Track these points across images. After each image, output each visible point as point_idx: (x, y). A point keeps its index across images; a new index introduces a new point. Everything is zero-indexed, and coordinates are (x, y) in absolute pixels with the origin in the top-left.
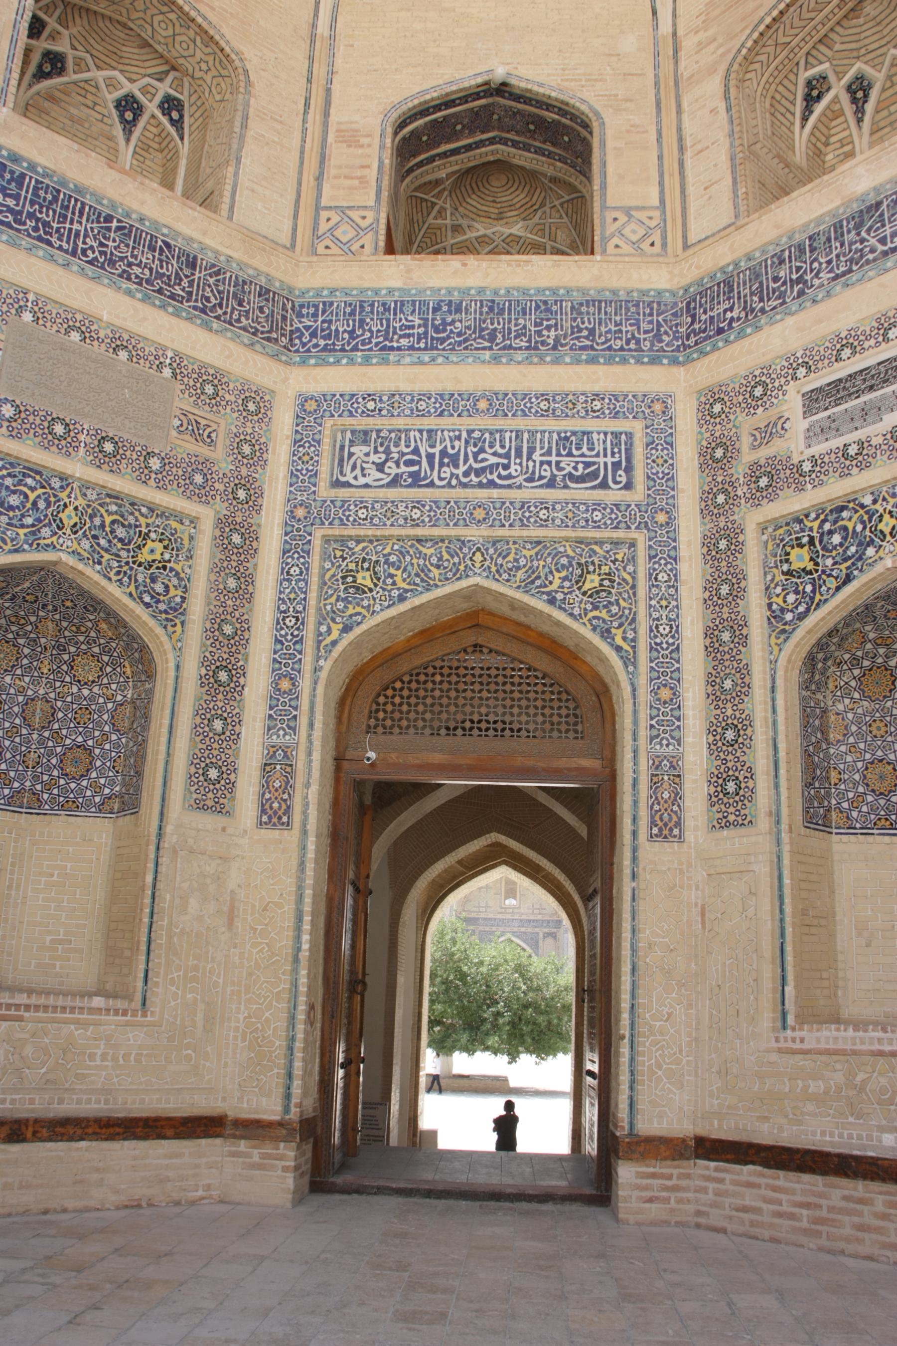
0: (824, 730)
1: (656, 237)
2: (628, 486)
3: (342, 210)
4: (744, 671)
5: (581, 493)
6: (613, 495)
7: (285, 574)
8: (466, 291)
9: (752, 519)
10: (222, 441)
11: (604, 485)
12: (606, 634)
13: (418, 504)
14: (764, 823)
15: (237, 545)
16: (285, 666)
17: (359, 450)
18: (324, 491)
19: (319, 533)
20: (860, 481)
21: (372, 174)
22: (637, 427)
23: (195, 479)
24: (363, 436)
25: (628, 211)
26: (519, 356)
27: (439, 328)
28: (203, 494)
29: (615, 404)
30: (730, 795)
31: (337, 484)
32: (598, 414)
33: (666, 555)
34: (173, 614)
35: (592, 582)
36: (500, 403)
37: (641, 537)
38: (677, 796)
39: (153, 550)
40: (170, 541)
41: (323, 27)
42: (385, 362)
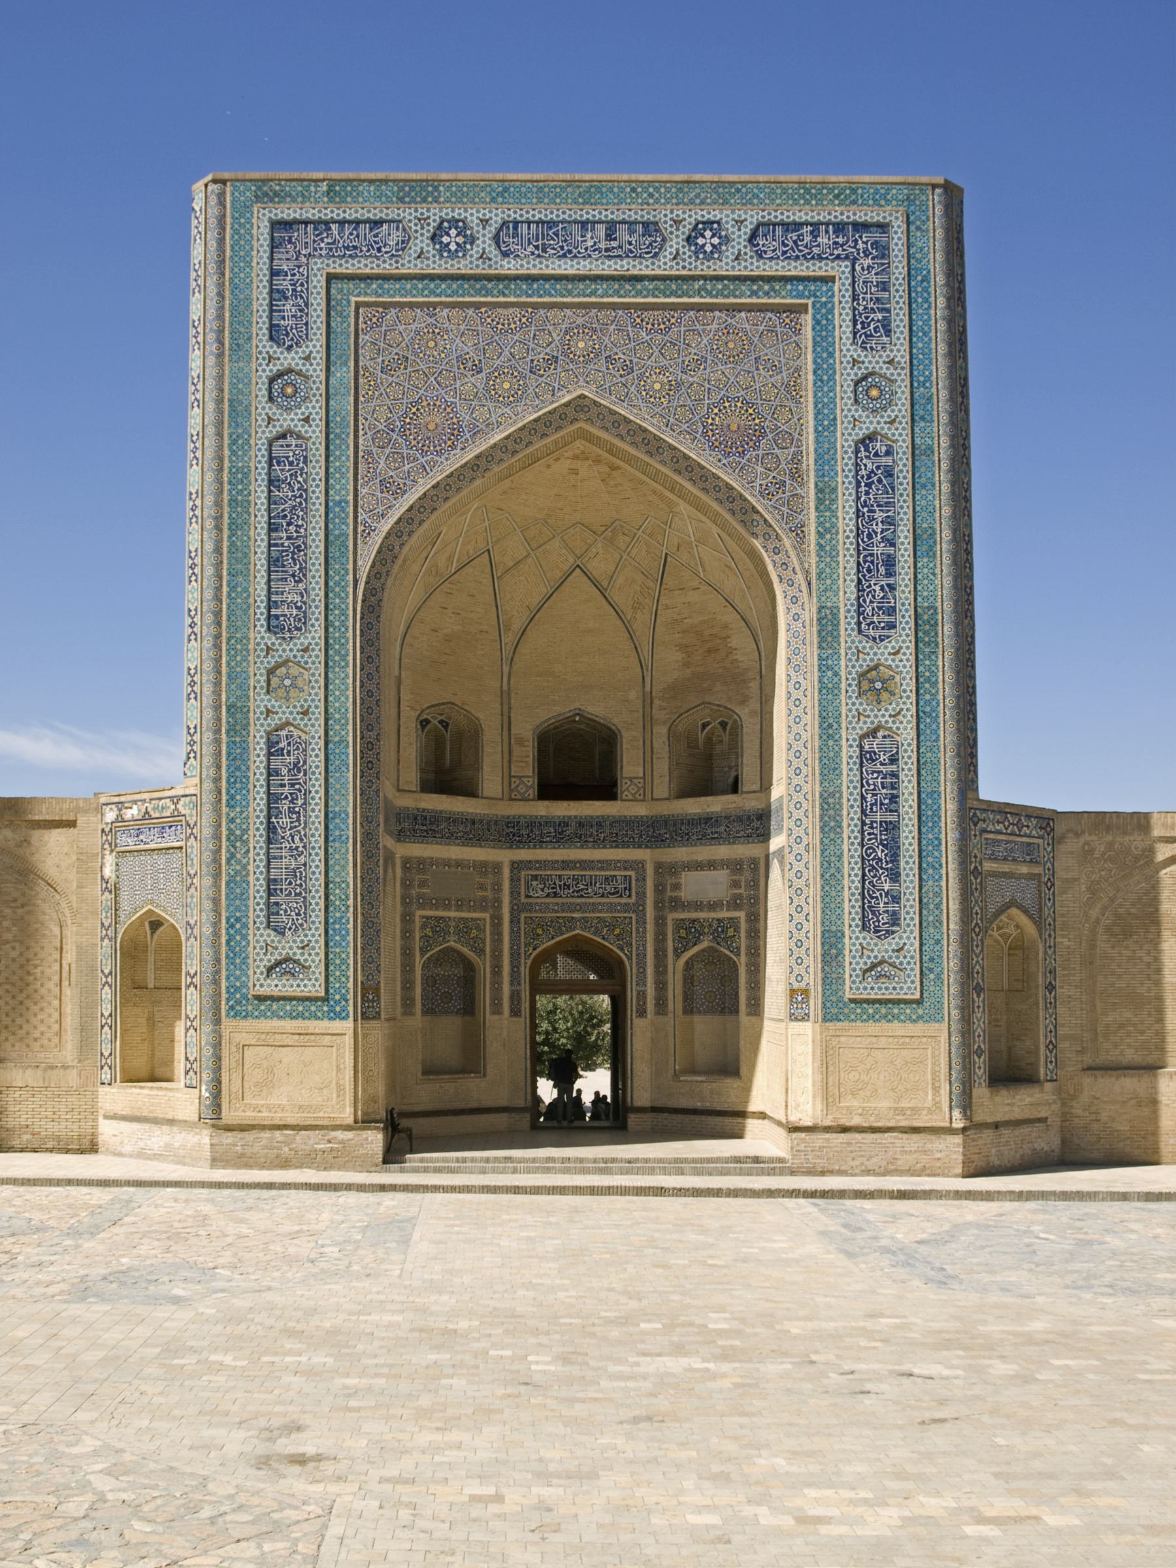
0: (692, 983)
1: (641, 792)
2: (630, 896)
3: (520, 777)
4: (666, 966)
5: (613, 899)
6: (623, 900)
7: (512, 931)
8: (570, 817)
9: (671, 917)
10: (489, 887)
11: (621, 896)
12: (622, 950)
13: (557, 904)
14: (671, 1015)
15: (497, 920)
16: (515, 966)
17: (535, 883)
18: (523, 900)
19: (523, 916)
20: (702, 915)
21: (531, 759)
22: (632, 873)
23: (481, 905)
24: (535, 877)
25: (631, 779)
26: (590, 845)
27: (562, 833)
29: (626, 865)
30: (661, 1006)
31: (528, 896)
32: (619, 869)
33: (642, 921)
34: (481, 952)
35: (617, 931)
36: (585, 864)
37: (633, 916)
38: (645, 1003)
39: (474, 932)
40: (478, 928)
41: (505, 687)
42: (541, 847)
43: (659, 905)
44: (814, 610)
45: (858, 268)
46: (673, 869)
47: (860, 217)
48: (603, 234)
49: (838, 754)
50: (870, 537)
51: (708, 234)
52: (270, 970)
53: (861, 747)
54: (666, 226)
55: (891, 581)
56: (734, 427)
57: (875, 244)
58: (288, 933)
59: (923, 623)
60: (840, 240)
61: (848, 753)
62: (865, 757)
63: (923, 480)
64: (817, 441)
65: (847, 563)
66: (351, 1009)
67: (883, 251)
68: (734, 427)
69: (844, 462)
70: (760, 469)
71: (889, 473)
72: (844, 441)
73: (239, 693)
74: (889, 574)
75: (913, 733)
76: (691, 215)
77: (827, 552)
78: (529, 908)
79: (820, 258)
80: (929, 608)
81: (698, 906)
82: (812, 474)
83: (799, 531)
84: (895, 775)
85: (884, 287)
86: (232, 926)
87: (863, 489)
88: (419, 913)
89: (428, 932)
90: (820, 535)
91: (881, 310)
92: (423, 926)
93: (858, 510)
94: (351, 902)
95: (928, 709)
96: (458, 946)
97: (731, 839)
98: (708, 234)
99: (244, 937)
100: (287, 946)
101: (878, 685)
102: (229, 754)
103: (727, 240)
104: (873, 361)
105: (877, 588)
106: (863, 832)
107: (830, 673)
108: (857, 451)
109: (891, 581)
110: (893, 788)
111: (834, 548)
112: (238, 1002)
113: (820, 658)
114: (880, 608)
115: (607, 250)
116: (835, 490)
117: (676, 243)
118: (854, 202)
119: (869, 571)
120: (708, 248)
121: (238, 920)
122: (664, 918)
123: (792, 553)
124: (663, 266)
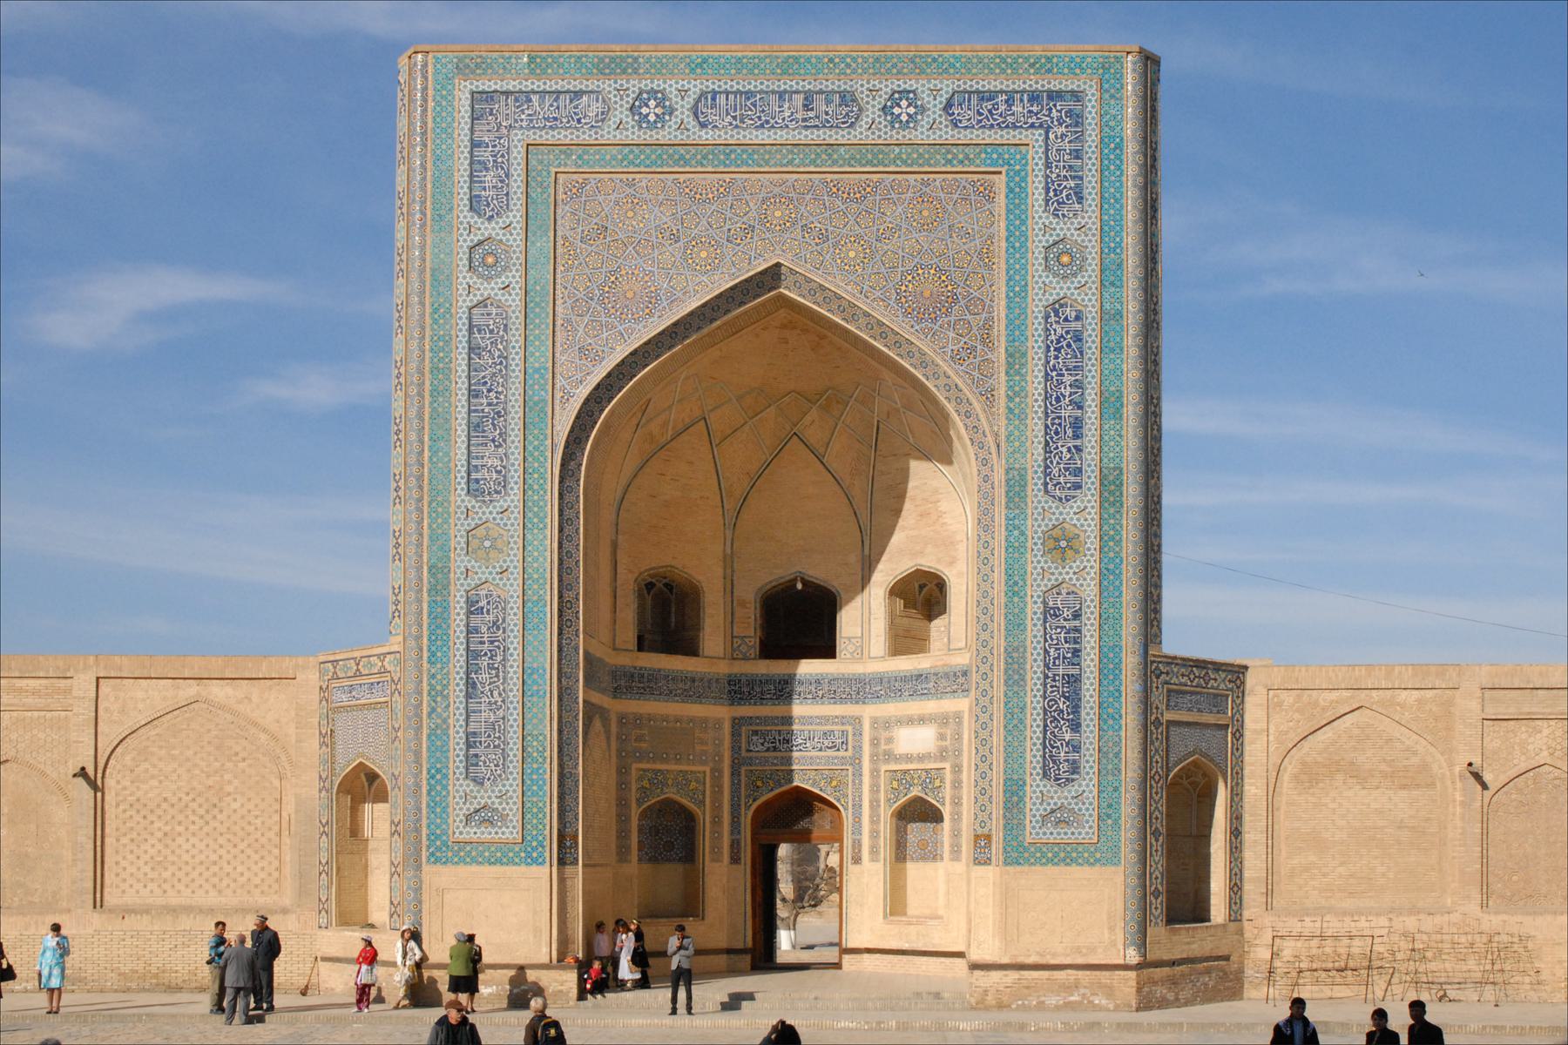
5: (830, 753)
7: (733, 784)
15: (717, 772)
18: (744, 754)
22: (850, 728)
24: (755, 733)
28: (704, 763)
29: (843, 720)
33: (858, 774)
43: (874, 758)
44: (1002, 471)
45: (1051, 136)
46: (887, 724)
47: (1055, 85)
48: (800, 104)
49: (1023, 610)
50: (1058, 400)
51: (904, 103)
52: (468, 818)
53: (1045, 603)
54: (863, 96)
55: (1078, 442)
56: (927, 294)
57: (1069, 113)
58: (487, 784)
59: (1110, 486)
60: (1035, 109)
61: (1033, 609)
62: (1050, 613)
63: (1111, 344)
64: (1009, 308)
65: (1035, 427)
66: (547, 854)
67: (1077, 119)
68: (927, 294)
69: (1035, 326)
70: (952, 335)
71: (1078, 339)
72: (1036, 307)
73: (440, 554)
74: (1076, 436)
75: (1096, 590)
76: (888, 86)
77: (1016, 414)
78: (750, 762)
79: (1015, 127)
80: (1115, 469)
81: (909, 758)
82: (1003, 339)
83: (989, 396)
84: (1077, 630)
85: (1077, 154)
86: (433, 777)
87: (1052, 353)
88: (635, 766)
89: (645, 783)
90: (1010, 398)
91: (1073, 178)
92: (640, 779)
93: (1047, 374)
94: (547, 754)
95: (1111, 567)
96: (677, 798)
97: (939, 694)
98: (904, 103)
99: (445, 787)
100: (484, 796)
101: (1063, 544)
102: (430, 614)
103: (922, 110)
104: (1062, 229)
105: (1064, 450)
106: (1045, 685)
107: (1016, 533)
108: (1047, 317)
109: (1078, 442)
110: (1076, 642)
111: (1023, 411)
112: (438, 849)
113: (1008, 519)
114: (1066, 469)
115: (804, 120)
116: (1024, 355)
117: (872, 112)
118: (1049, 71)
119: (1057, 433)
120: (904, 118)
121: (438, 771)
122: (878, 771)
123: (982, 417)
124: (860, 134)
